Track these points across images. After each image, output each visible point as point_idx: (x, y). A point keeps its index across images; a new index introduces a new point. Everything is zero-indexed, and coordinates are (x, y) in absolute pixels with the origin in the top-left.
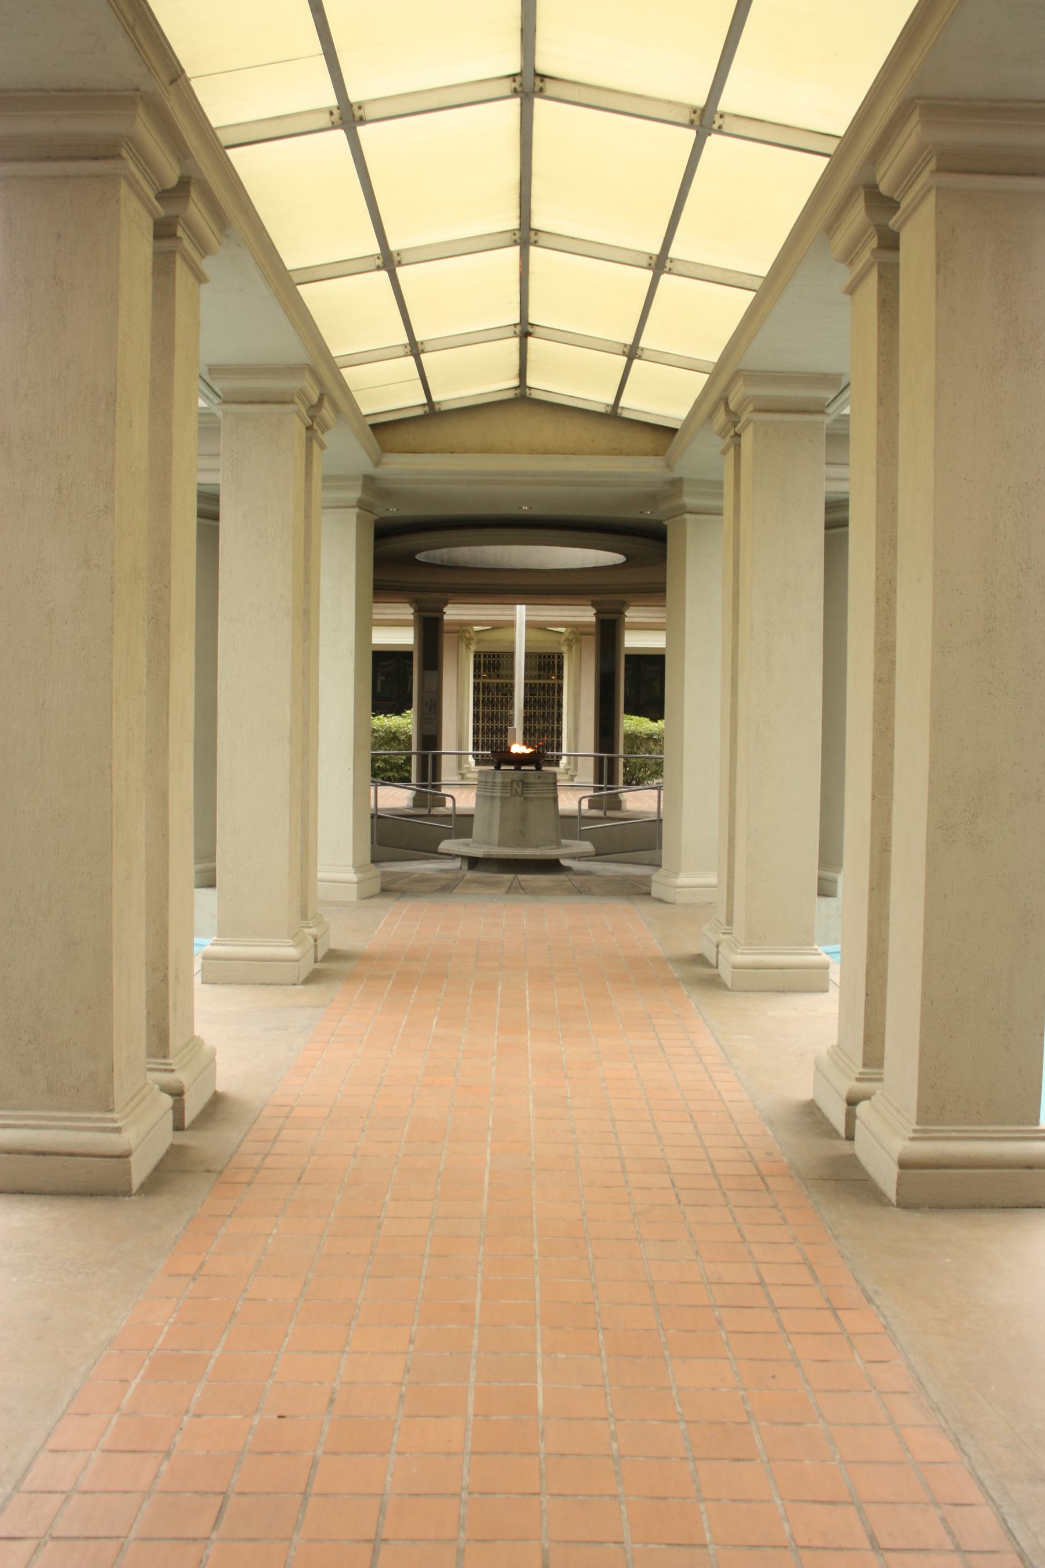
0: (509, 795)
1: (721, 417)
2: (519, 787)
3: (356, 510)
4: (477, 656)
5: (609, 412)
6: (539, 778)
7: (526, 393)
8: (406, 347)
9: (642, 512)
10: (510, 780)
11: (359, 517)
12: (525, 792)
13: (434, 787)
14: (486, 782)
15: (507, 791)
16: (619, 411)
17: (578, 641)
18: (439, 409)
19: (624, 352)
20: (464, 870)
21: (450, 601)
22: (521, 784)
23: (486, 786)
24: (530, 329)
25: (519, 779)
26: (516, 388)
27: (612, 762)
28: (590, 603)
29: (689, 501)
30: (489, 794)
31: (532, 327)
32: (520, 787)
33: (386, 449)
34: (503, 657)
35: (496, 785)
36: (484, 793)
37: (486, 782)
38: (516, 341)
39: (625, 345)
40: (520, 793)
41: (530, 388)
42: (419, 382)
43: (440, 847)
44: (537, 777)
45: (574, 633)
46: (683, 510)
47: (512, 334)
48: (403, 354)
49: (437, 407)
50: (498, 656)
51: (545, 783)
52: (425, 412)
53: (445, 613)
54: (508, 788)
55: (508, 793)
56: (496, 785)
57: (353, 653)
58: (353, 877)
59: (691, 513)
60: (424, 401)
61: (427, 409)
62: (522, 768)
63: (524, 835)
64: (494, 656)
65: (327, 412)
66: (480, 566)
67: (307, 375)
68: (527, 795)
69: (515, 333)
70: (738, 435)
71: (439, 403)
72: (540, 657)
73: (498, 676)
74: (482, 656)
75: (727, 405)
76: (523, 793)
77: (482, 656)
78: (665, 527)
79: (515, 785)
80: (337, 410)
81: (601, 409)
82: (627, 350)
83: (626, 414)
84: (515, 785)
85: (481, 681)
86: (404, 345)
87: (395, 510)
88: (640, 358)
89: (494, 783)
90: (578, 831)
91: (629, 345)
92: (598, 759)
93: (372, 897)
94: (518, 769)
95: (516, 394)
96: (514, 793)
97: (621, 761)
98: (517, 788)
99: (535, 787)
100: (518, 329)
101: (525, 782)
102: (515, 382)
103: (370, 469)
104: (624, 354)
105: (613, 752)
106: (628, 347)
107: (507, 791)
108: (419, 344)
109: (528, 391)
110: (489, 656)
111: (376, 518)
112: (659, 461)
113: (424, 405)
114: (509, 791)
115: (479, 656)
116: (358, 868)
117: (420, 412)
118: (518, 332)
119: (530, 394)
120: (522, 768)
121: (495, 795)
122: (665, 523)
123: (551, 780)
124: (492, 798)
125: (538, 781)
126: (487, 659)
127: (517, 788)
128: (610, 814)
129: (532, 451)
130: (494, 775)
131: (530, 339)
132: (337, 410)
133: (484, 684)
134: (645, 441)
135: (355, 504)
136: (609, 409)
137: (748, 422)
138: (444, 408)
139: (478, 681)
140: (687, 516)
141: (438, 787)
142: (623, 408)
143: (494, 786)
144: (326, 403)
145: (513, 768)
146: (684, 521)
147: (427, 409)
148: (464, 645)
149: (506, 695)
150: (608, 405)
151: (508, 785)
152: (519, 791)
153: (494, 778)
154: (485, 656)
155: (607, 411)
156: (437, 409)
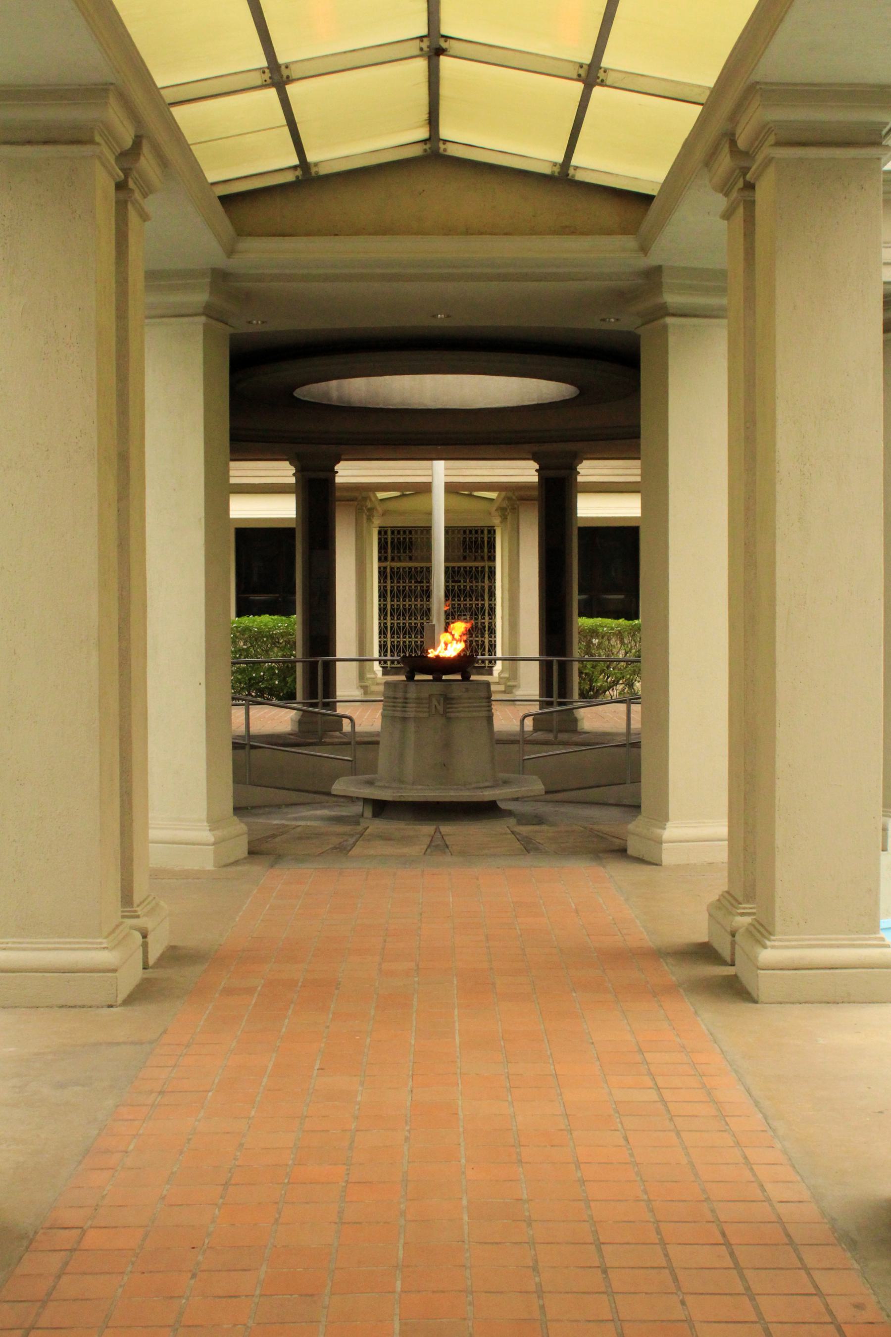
0: (426, 715)
1: (725, 162)
2: (439, 705)
3: (203, 319)
4: (382, 532)
5: (556, 174)
6: (467, 690)
7: (439, 148)
8: (264, 72)
9: (604, 320)
10: (427, 695)
11: (208, 332)
12: (448, 710)
13: (326, 705)
15: (425, 709)
16: (571, 171)
17: (515, 510)
18: (317, 172)
19: (579, 75)
20: (367, 818)
21: (343, 457)
24: (444, 45)
26: (424, 141)
27: (564, 668)
28: (531, 457)
29: (671, 299)
30: (398, 714)
31: (446, 41)
33: (242, 232)
34: (416, 532)
35: (408, 701)
38: (421, 64)
39: (581, 66)
40: (442, 713)
41: (445, 141)
42: (286, 130)
43: (333, 787)
44: (464, 690)
45: (509, 499)
46: (663, 311)
47: (417, 52)
48: (259, 83)
49: (313, 170)
50: (410, 532)
52: (297, 177)
53: (337, 472)
55: (425, 712)
56: (408, 701)
57: (203, 521)
58: (207, 836)
59: (674, 315)
60: (295, 161)
61: (299, 172)
62: (444, 677)
64: (404, 532)
65: (147, 163)
66: (381, 406)
67: (112, 100)
69: (421, 49)
70: (750, 187)
71: (316, 164)
72: (465, 532)
73: (411, 558)
74: (389, 533)
75: (733, 142)
76: (445, 712)
77: (389, 533)
78: (639, 337)
79: (435, 702)
80: (164, 163)
81: (546, 170)
82: (583, 72)
83: (580, 176)
84: (435, 702)
85: (388, 564)
86: (260, 69)
87: (260, 322)
88: (602, 84)
89: (406, 699)
90: (521, 760)
91: (586, 64)
92: (545, 663)
93: (236, 863)
94: (438, 679)
95: (425, 150)
97: (576, 666)
99: (461, 703)
100: (425, 44)
102: (423, 133)
103: (219, 259)
104: (579, 78)
105: (564, 656)
106: (585, 67)
107: (425, 709)
108: (283, 68)
109: (442, 146)
110: (399, 532)
111: (231, 330)
112: (629, 242)
113: (295, 168)
115: (386, 533)
116: (214, 823)
117: (290, 177)
118: (425, 49)
119: (445, 150)
120: (444, 677)
121: (407, 715)
122: (638, 332)
123: (483, 694)
124: (404, 719)
126: (396, 536)
128: (563, 737)
129: (448, 231)
131: (443, 59)
132: (164, 163)
133: (392, 568)
134: (606, 213)
135: (201, 310)
136: (557, 170)
137: (769, 161)
138: (324, 170)
139: (384, 564)
140: (669, 320)
141: (332, 706)
142: (576, 168)
143: (406, 703)
144: (146, 149)
145: (430, 677)
146: (665, 327)
147: (299, 172)
148: (365, 517)
149: (423, 582)
150: (555, 164)
151: (424, 701)
152: (441, 709)
153: (406, 692)
154: (393, 533)
155: (553, 172)
156: (313, 174)
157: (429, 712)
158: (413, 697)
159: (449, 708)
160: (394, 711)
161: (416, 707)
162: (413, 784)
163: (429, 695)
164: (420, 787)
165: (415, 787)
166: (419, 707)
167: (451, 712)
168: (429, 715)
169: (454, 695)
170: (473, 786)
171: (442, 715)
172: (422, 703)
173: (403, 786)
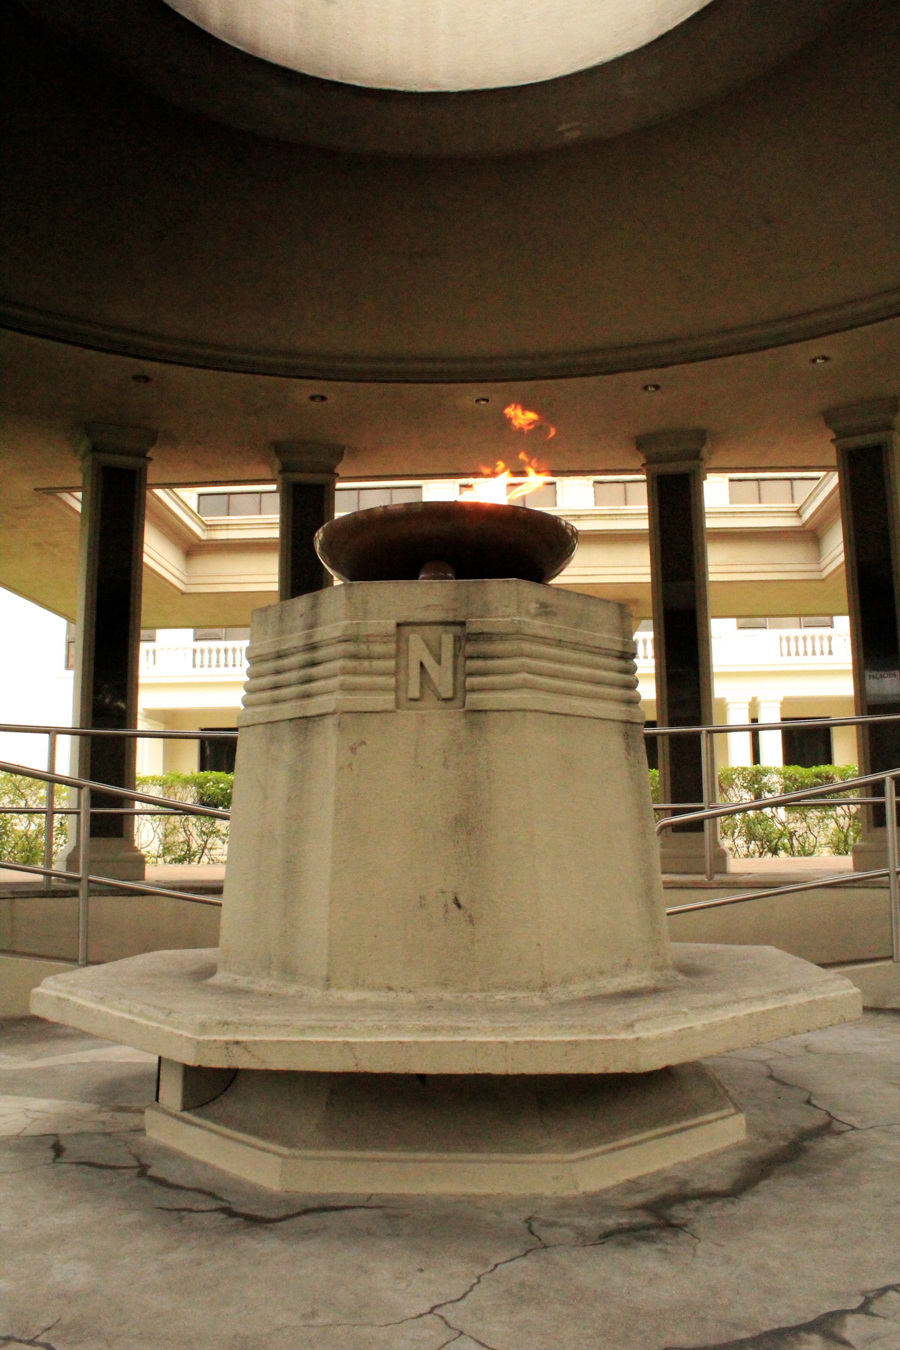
0: (386, 700)
2: (439, 662)
10: (390, 625)
12: (471, 681)
14: (280, 656)
20: (164, 1111)
22: (448, 640)
23: (278, 672)
30: (287, 710)
32: (447, 654)
35: (320, 654)
36: (266, 708)
44: (533, 607)
54: (379, 664)
55: (384, 689)
56: (320, 654)
63: (471, 920)
66: (335, 78)
68: (473, 699)
76: (461, 690)
89: (313, 647)
96: (414, 692)
98: (430, 663)
114: (392, 681)
125: (538, 626)
127: (430, 663)
128: (717, 877)
143: (313, 664)
151: (378, 648)
157: (396, 689)
158: (337, 634)
159: (471, 674)
160: (276, 702)
161: (344, 671)
162: (328, 982)
163: (399, 625)
164: (352, 996)
165: (336, 994)
166: (355, 672)
167: (482, 689)
169: (495, 622)
170: (580, 988)
171: (447, 700)
173: (292, 989)
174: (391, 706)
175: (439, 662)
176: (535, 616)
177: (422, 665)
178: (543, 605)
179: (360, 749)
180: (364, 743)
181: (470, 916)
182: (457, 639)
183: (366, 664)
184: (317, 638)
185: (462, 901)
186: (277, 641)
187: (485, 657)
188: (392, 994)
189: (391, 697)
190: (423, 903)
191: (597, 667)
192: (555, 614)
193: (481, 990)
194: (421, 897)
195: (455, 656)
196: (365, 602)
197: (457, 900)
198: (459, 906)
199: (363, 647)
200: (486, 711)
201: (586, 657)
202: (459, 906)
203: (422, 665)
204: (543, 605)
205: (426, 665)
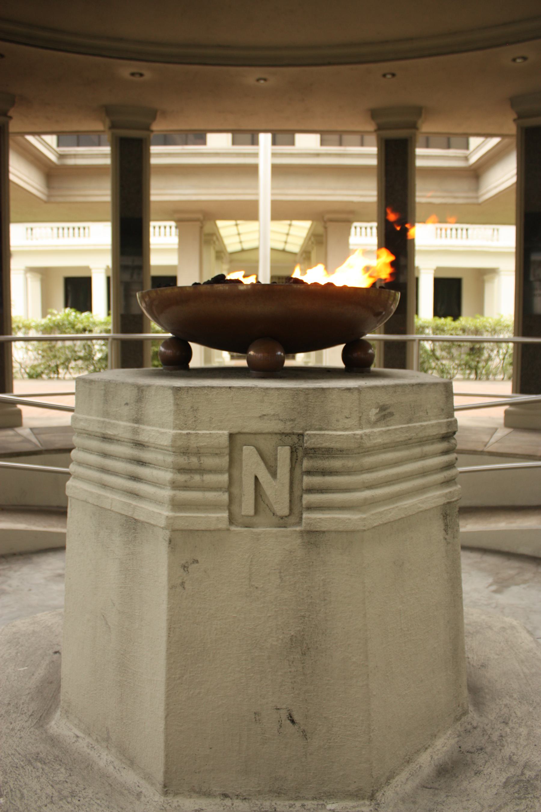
2: (274, 474)
12: (308, 498)
14: (105, 438)
15: (211, 496)
22: (284, 453)
23: (105, 455)
25: (278, 427)
37: (105, 438)
40: (282, 508)
44: (373, 413)
51: (407, 444)
54: (210, 478)
56: (146, 455)
63: (304, 735)
89: (139, 445)
101: (308, 443)
130: (140, 400)
143: (141, 463)
151: (209, 462)
159: (310, 491)
160: (104, 486)
166: (185, 487)
168: (231, 520)
172: (201, 471)
174: (224, 525)
175: (274, 474)
176: (375, 424)
177: (256, 478)
178: (383, 408)
179: (193, 567)
180: (197, 562)
181: (304, 731)
182: (293, 451)
183: (197, 478)
184: (143, 438)
185: (296, 718)
186: (103, 422)
187: (324, 473)
188: (228, 802)
189: (225, 515)
190: (257, 718)
191: (424, 457)
192: (391, 414)
193: (314, 798)
194: (255, 713)
195: (292, 470)
196: (195, 410)
197: (291, 717)
198: (293, 722)
199: (194, 460)
200: (324, 532)
201: (417, 451)
202: (293, 722)
203: (256, 478)
204: (383, 408)
205: (261, 480)
